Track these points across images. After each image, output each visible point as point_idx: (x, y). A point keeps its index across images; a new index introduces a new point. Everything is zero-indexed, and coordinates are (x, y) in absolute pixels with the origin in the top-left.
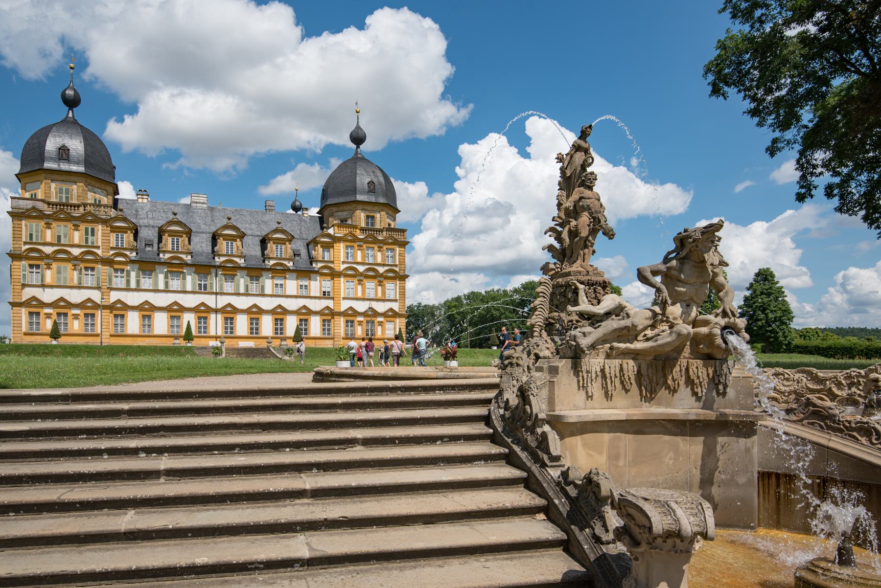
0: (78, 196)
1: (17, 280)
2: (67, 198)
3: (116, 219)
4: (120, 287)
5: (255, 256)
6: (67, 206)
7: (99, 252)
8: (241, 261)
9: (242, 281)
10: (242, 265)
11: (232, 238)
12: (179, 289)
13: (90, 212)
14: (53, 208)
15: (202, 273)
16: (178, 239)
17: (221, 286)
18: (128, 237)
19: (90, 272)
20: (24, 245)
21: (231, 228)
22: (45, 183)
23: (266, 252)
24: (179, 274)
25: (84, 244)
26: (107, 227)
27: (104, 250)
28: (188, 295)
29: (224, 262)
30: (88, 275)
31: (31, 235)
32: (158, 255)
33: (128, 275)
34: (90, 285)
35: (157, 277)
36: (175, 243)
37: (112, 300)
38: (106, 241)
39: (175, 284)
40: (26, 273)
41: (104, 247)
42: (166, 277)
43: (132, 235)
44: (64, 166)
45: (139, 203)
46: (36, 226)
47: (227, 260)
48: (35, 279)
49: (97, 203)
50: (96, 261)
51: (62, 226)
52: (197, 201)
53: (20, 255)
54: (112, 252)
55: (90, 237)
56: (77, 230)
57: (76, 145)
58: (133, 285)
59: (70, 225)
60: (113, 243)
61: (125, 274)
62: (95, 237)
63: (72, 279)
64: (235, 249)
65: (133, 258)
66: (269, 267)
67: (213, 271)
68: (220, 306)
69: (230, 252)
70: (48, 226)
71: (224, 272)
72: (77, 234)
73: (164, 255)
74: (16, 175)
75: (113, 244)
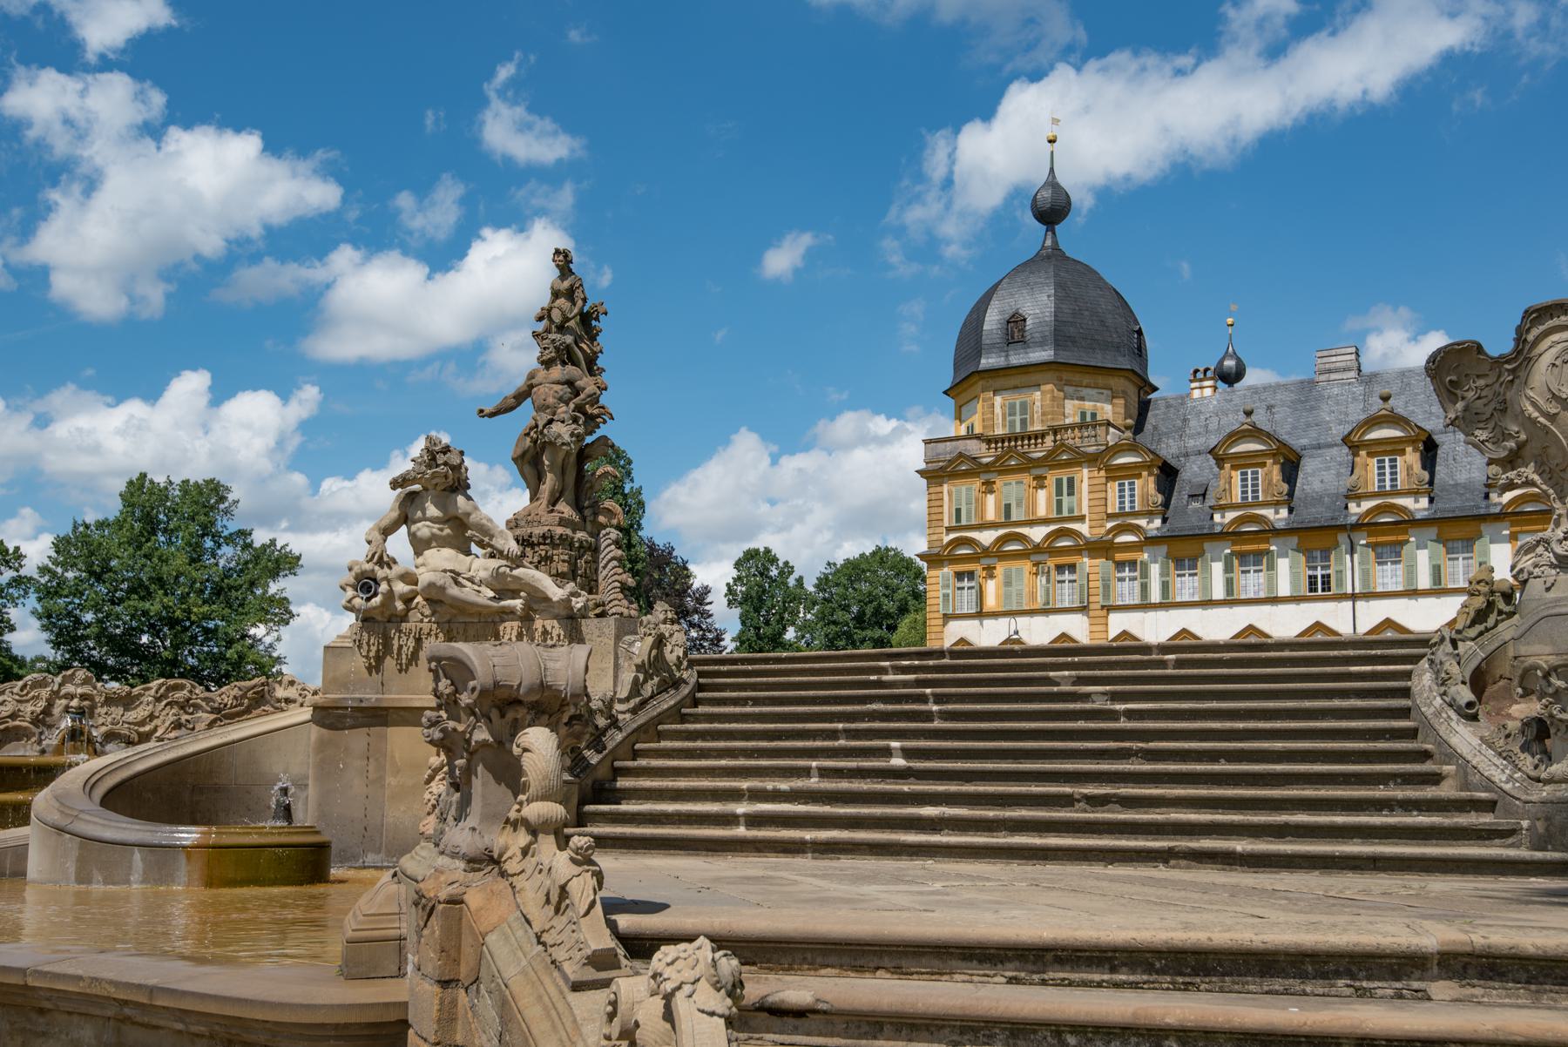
0: (1043, 414)
1: (935, 608)
2: (1024, 422)
3: (1118, 449)
4: (1127, 603)
5: (1468, 487)
7: (1083, 528)
8: (1419, 506)
9: (1423, 559)
10: (1418, 516)
11: (1392, 448)
12: (1262, 595)
13: (1063, 445)
14: (996, 449)
15: (1316, 549)
16: (1257, 473)
17: (1366, 575)
18: (1146, 486)
19: (1067, 576)
20: (947, 534)
21: (1388, 422)
22: (983, 401)
24: (1260, 557)
25: (1055, 516)
26: (1100, 469)
27: (1094, 523)
28: (1282, 608)
29: (1369, 512)
30: (1064, 582)
31: (958, 511)
32: (1212, 518)
33: (1145, 574)
34: (1067, 605)
35: (1208, 571)
36: (1250, 482)
37: (1113, 632)
38: (1097, 503)
39: (1252, 582)
40: (950, 591)
41: (1094, 517)
42: (1228, 569)
43: (1152, 479)
44: (1016, 359)
45: (1195, 400)
46: (957, 493)
47: (1377, 507)
48: (966, 602)
49: (1088, 419)
51: (1014, 482)
52: (1332, 366)
53: (937, 554)
54: (1109, 525)
55: (1065, 498)
56: (1042, 487)
57: (1038, 305)
58: (1155, 596)
59: (1027, 478)
60: (1114, 505)
61: (1137, 574)
62: (1075, 498)
63: (1033, 596)
65: (1155, 533)
66: (1497, 510)
67: (1342, 538)
68: (1364, 627)
69: (1388, 483)
70: (989, 487)
71: (1373, 540)
72: (1042, 495)
73: (1223, 517)
74: (945, 393)
75: (1113, 507)
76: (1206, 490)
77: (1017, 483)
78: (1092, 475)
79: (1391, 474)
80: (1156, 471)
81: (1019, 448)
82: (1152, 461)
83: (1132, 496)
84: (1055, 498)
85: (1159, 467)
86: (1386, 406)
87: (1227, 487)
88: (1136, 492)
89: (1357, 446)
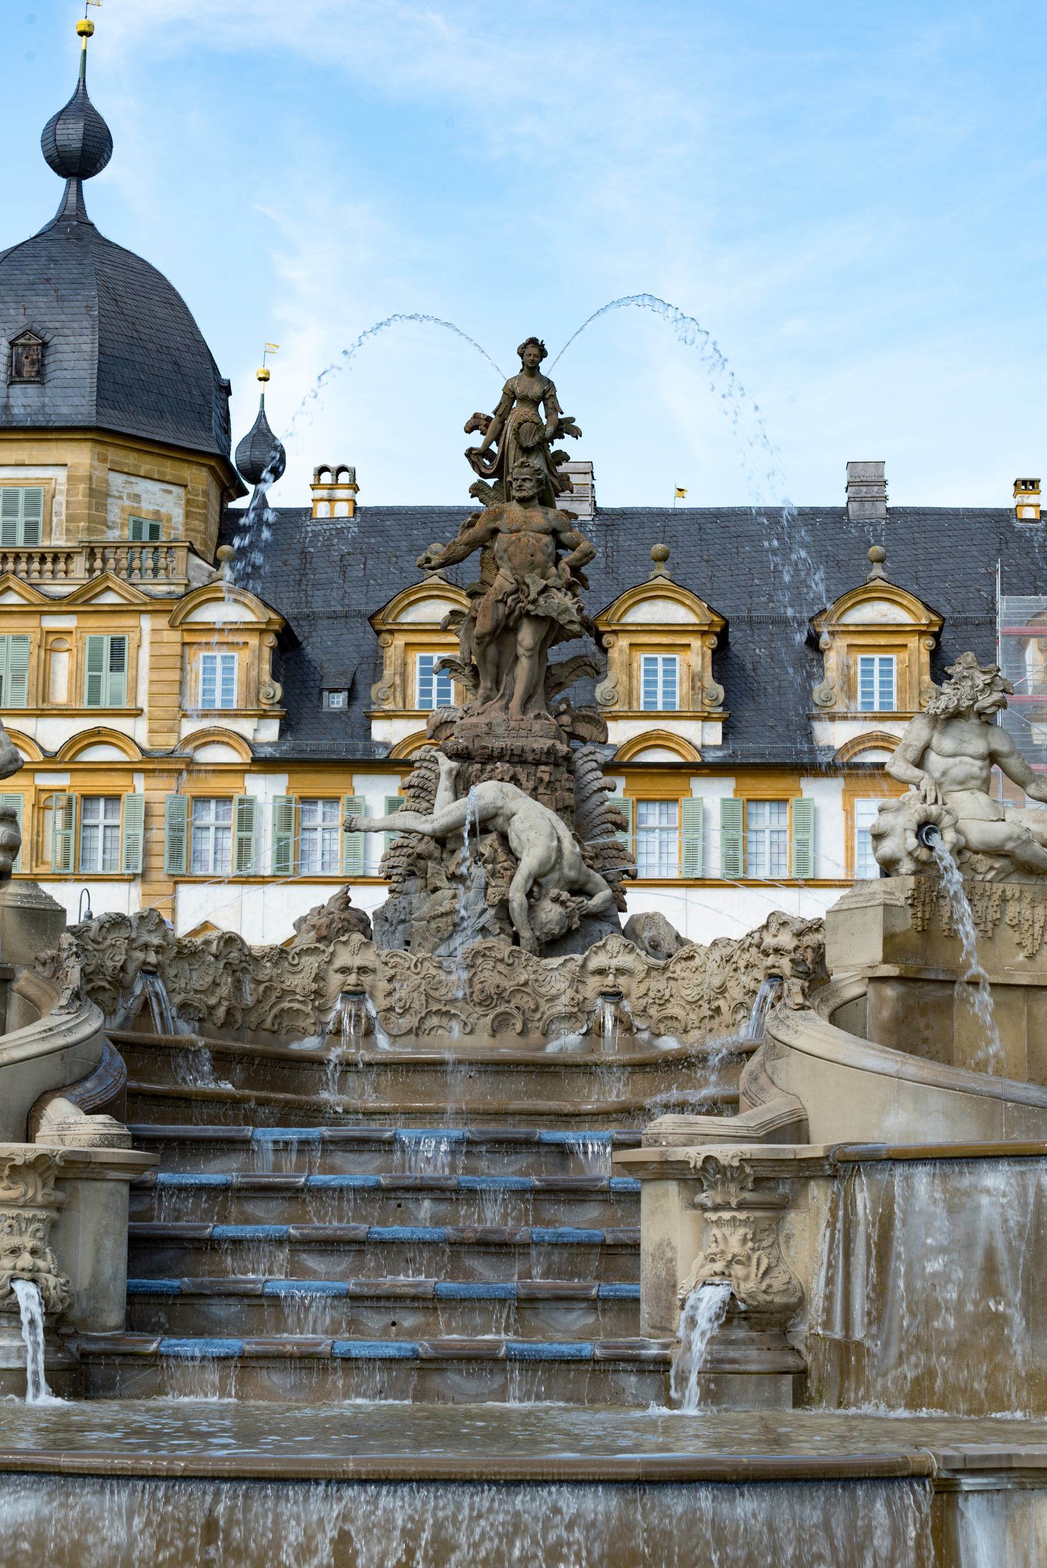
0: (70, 518)
2: (31, 529)
6: (30, 558)
7: (139, 730)
10: (711, 757)
23: (819, 691)
25: (85, 706)
27: (157, 725)
29: (632, 743)
38: (166, 689)
41: (159, 713)
43: (267, 654)
47: (645, 737)
50: (128, 770)
55: (107, 678)
61: (232, 821)
64: (681, 689)
65: (267, 752)
69: (660, 699)
76: (354, 683)
77: (16, 639)
78: (158, 638)
79: (666, 683)
80: (271, 640)
81: (23, 575)
82: (269, 622)
83: (227, 681)
84: (87, 674)
85: (277, 635)
86: (664, 572)
87: (398, 681)
88: (236, 676)
89: (615, 632)
